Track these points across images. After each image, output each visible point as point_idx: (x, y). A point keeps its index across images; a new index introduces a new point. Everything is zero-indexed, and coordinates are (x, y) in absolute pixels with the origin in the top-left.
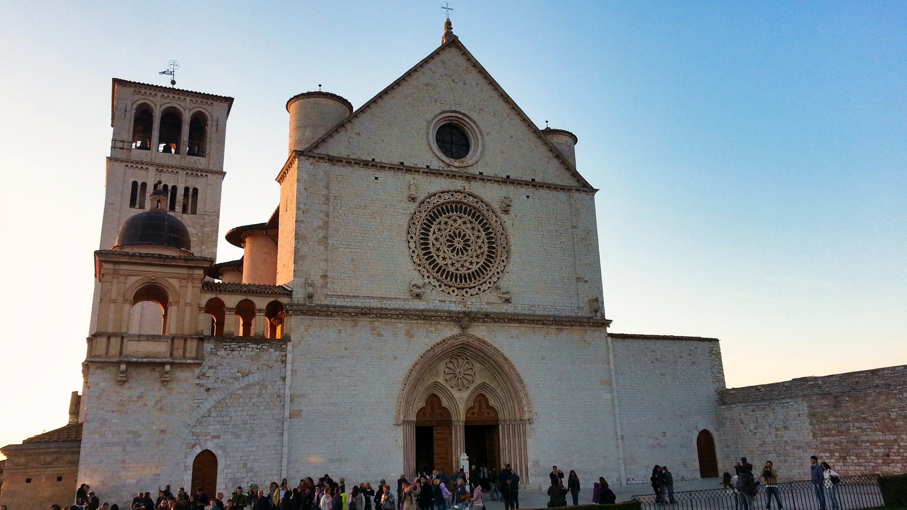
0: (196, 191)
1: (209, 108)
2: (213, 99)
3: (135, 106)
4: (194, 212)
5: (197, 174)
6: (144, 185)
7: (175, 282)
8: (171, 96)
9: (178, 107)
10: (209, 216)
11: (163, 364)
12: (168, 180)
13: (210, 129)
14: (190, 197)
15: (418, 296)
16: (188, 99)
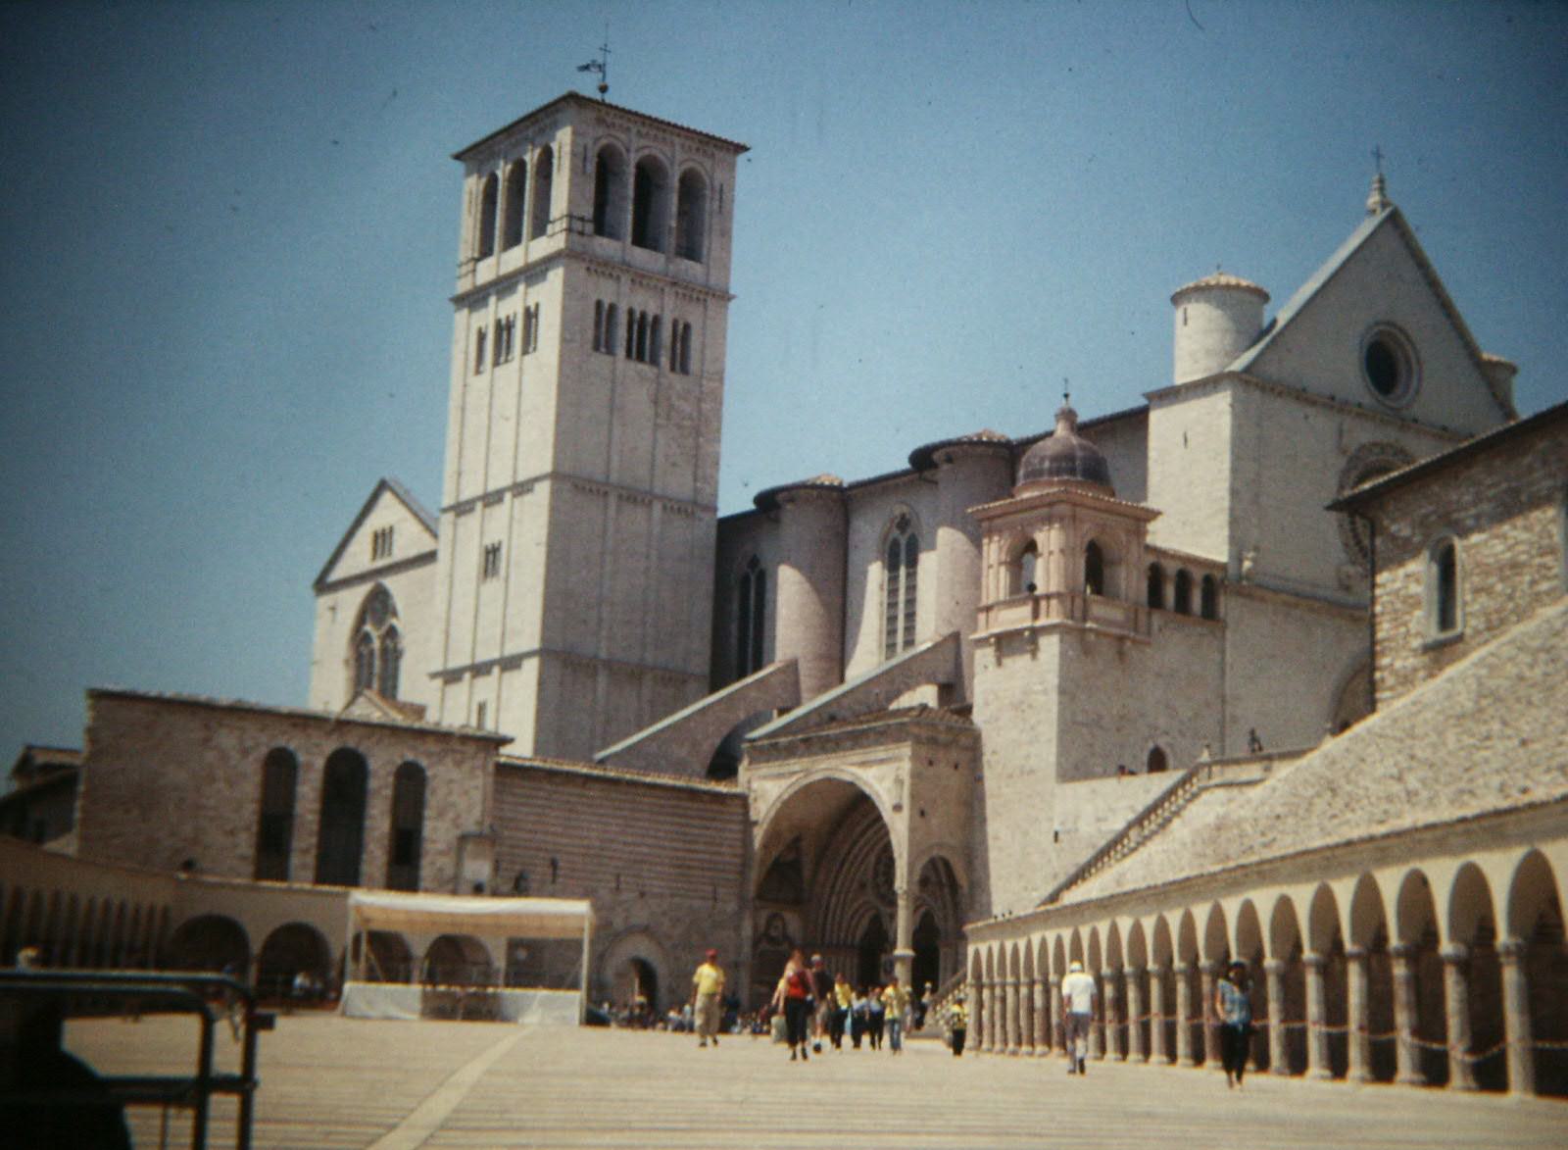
0: (687, 327)
1: (708, 164)
2: (715, 146)
3: (596, 149)
4: (685, 371)
5: (691, 297)
6: (612, 308)
7: (1123, 538)
8: (653, 132)
9: (661, 156)
10: (710, 380)
11: (1121, 639)
12: (646, 302)
13: (710, 205)
14: (679, 338)
15: (1347, 589)
16: (677, 140)
